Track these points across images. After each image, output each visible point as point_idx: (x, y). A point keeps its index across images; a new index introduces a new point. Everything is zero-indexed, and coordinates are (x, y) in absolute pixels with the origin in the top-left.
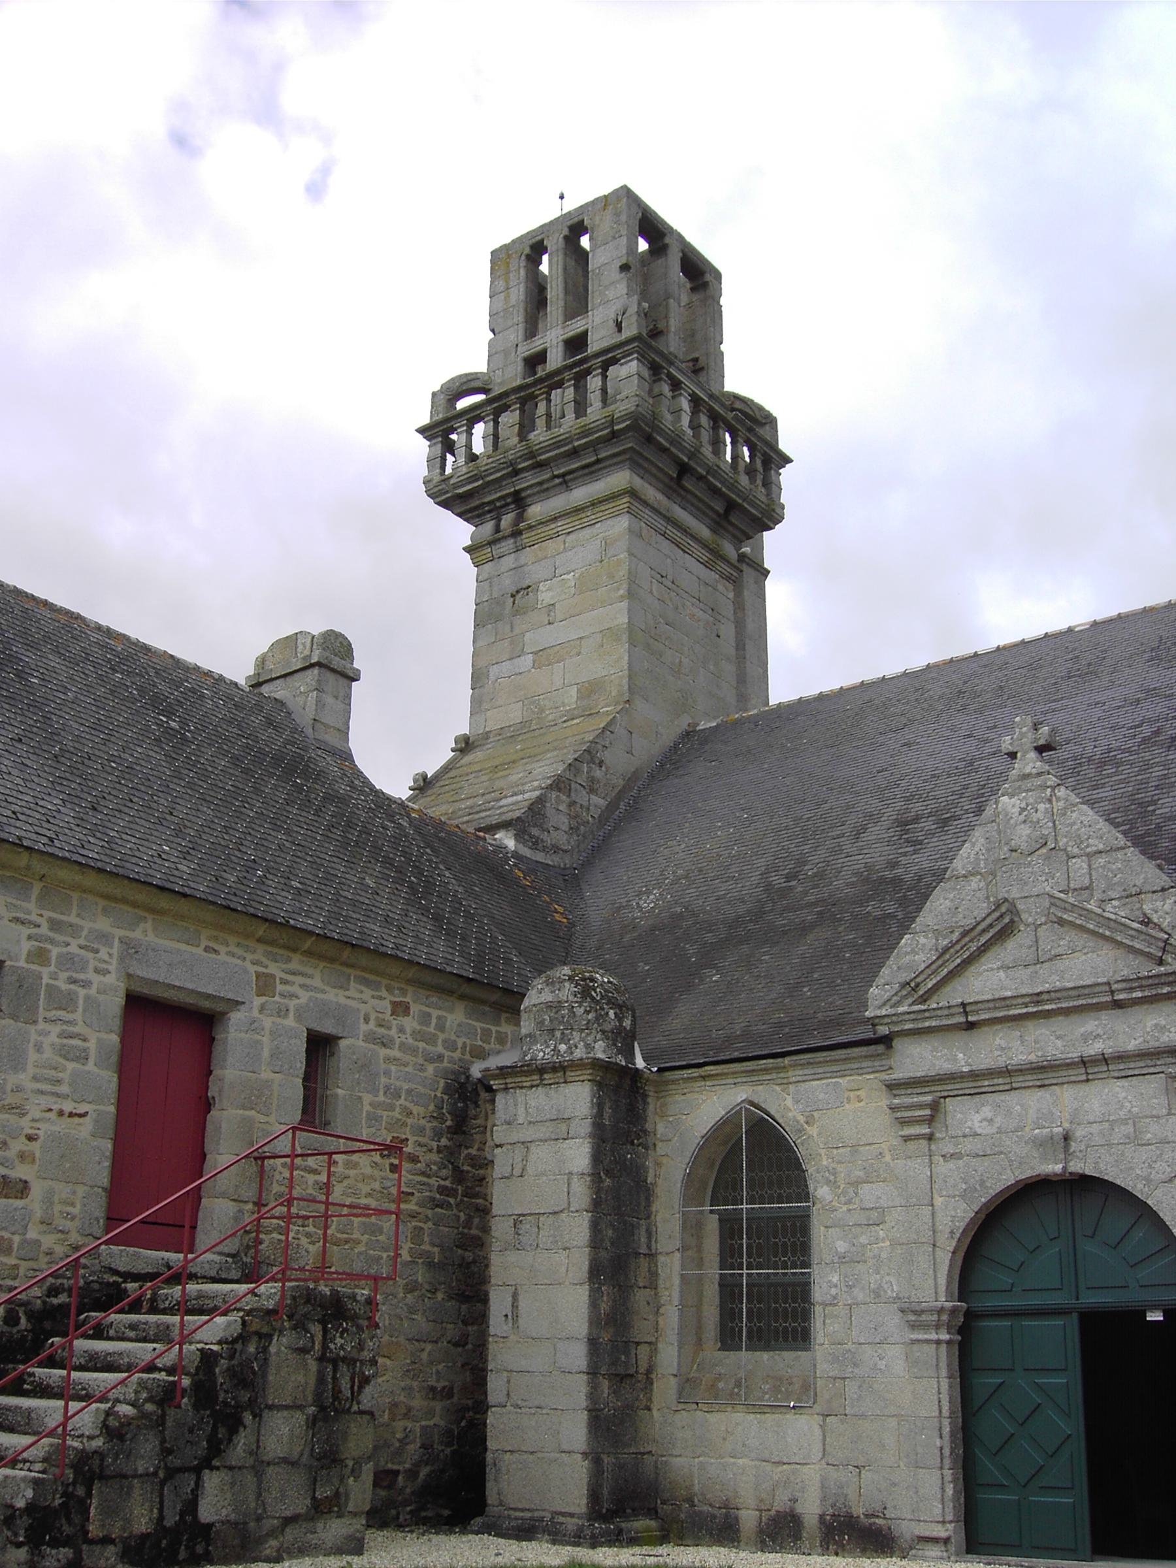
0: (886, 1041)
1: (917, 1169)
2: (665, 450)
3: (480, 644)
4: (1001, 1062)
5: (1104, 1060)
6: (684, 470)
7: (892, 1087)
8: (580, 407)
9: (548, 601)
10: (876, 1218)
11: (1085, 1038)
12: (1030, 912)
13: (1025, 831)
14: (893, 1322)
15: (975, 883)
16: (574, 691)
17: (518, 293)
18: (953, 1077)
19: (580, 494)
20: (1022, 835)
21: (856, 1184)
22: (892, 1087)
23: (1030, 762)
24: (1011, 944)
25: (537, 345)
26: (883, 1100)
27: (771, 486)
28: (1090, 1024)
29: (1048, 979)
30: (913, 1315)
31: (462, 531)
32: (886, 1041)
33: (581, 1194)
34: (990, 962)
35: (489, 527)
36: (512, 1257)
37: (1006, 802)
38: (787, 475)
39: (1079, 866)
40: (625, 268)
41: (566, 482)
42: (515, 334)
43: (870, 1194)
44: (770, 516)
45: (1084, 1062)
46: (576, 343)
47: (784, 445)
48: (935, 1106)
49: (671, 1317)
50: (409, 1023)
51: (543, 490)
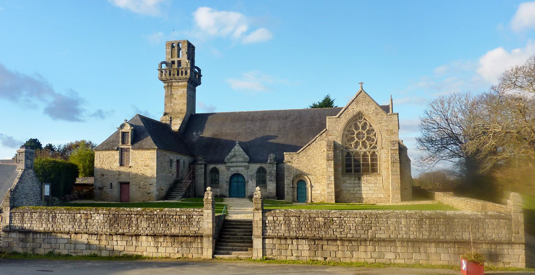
0: (226, 163)
1: (227, 172)
2: (191, 80)
4: (234, 165)
5: (241, 166)
6: (192, 81)
7: (226, 166)
9: (175, 97)
10: (224, 175)
11: (240, 164)
12: (237, 155)
13: (237, 149)
14: (225, 183)
15: (233, 153)
16: (179, 109)
18: (231, 166)
19: (180, 84)
21: (223, 173)
22: (226, 166)
23: (238, 144)
24: (235, 157)
26: (225, 167)
28: (240, 163)
29: (238, 160)
30: (227, 182)
31: (163, 84)
32: (226, 163)
33: (203, 173)
34: (234, 158)
36: (197, 178)
38: (202, 77)
39: (240, 152)
40: (186, 53)
41: (178, 82)
43: (224, 174)
45: (240, 166)
48: (229, 168)
50: (188, 159)
51: (175, 82)
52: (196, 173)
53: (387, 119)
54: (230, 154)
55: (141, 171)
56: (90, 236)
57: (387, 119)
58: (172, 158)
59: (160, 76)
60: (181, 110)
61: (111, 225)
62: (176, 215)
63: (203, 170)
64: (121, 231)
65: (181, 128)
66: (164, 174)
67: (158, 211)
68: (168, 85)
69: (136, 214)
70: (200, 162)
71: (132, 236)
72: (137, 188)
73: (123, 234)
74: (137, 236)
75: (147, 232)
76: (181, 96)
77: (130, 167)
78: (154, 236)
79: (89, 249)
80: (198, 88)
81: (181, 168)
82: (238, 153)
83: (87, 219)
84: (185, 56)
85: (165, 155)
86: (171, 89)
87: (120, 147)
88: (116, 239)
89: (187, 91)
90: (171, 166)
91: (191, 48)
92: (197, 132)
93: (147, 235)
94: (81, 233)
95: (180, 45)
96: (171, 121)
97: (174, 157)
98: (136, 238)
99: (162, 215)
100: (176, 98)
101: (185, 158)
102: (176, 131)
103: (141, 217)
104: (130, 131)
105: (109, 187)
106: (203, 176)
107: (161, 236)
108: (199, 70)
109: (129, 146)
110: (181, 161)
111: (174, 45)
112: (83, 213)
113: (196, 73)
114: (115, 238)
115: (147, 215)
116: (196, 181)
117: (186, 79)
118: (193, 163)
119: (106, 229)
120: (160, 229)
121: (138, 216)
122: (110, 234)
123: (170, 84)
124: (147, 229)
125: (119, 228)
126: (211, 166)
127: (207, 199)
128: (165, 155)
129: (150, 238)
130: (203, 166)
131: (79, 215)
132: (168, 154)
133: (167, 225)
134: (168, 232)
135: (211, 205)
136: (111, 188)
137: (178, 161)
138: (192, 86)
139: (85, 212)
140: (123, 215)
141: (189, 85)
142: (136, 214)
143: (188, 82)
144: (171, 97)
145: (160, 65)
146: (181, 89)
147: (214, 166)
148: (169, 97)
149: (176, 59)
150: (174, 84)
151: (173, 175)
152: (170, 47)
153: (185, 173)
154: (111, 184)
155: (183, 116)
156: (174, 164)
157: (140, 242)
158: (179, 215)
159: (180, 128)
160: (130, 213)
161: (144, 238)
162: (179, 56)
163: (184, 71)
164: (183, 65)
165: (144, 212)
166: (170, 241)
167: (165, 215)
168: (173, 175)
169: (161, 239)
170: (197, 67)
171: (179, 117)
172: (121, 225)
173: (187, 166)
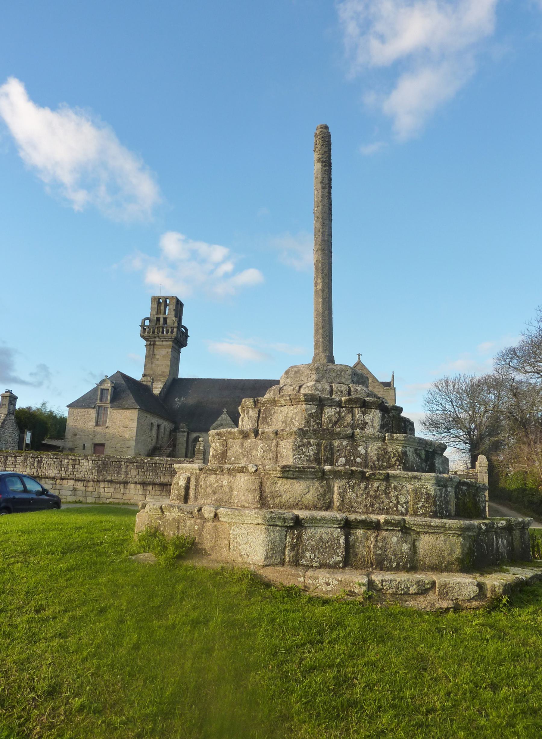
3: (147, 360)
6: (178, 341)
8: (167, 333)
17: (156, 306)
19: (164, 343)
20: (224, 418)
23: (225, 412)
25: (159, 316)
27: (186, 340)
31: (144, 342)
35: (149, 343)
37: (223, 415)
40: (174, 310)
41: (162, 341)
42: (155, 313)
44: (185, 345)
46: (165, 320)
47: (189, 335)
49: (190, 452)
51: (159, 341)
52: (178, 442)
53: (384, 393)
54: (216, 422)
55: (118, 432)
56: (77, 482)
57: (384, 393)
58: (153, 421)
59: (142, 333)
60: (163, 372)
61: (99, 472)
62: (167, 464)
63: (185, 439)
64: (109, 478)
65: (162, 393)
66: (143, 438)
67: (149, 459)
68: (150, 344)
69: (127, 462)
70: (182, 430)
71: (120, 483)
72: (113, 450)
73: (111, 481)
74: (126, 483)
75: (135, 480)
76: (164, 357)
77: (107, 427)
78: (144, 484)
79: (74, 496)
80: (183, 350)
81: (161, 435)
82: (225, 422)
83: (75, 465)
84: (172, 313)
85: (146, 417)
86: (154, 348)
87: (98, 404)
88: (103, 486)
89: (172, 351)
90: (151, 430)
91: (179, 305)
92: (180, 398)
93: (136, 483)
94: (67, 479)
95: (168, 301)
96: (153, 382)
97: (156, 421)
98: (124, 485)
99: (152, 464)
100: (158, 359)
101: (167, 423)
102: (156, 395)
103: (131, 465)
104: (110, 388)
105: (82, 448)
106: (185, 445)
107: (150, 484)
108: (186, 330)
109: (109, 405)
110: (162, 427)
111: (161, 300)
112: (71, 459)
113: (182, 332)
114: (102, 485)
115: (137, 462)
116: (177, 450)
117: (171, 338)
118: (175, 430)
119: (94, 476)
120: (149, 477)
121: (128, 464)
122: (98, 481)
123: (152, 343)
124: (136, 477)
125: (107, 475)
126: (194, 435)
127: (199, 449)
128: (146, 417)
129: (138, 486)
130: (186, 434)
131: (66, 461)
132: (149, 416)
133: (156, 473)
134: (157, 481)
135: (202, 455)
136: (84, 449)
137: (159, 426)
138: (177, 347)
139: (73, 458)
140: (113, 462)
141: (174, 345)
142: (127, 462)
143: (173, 342)
144: (153, 358)
145: (143, 321)
146: (165, 349)
147: (198, 435)
148: (150, 357)
149: (162, 316)
150: (157, 343)
151: (152, 440)
152: (156, 303)
153: (165, 439)
154: (84, 444)
155: (164, 379)
156: (155, 429)
157: (128, 490)
158: (170, 464)
159: (161, 392)
160: (120, 460)
161: (133, 486)
162: (165, 313)
163: (170, 330)
164: (170, 323)
165: (134, 460)
166: (158, 489)
167: (155, 464)
168: (152, 440)
169: (150, 488)
170: (185, 327)
171: (160, 380)
172: (109, 472)
173: (167, 432)
